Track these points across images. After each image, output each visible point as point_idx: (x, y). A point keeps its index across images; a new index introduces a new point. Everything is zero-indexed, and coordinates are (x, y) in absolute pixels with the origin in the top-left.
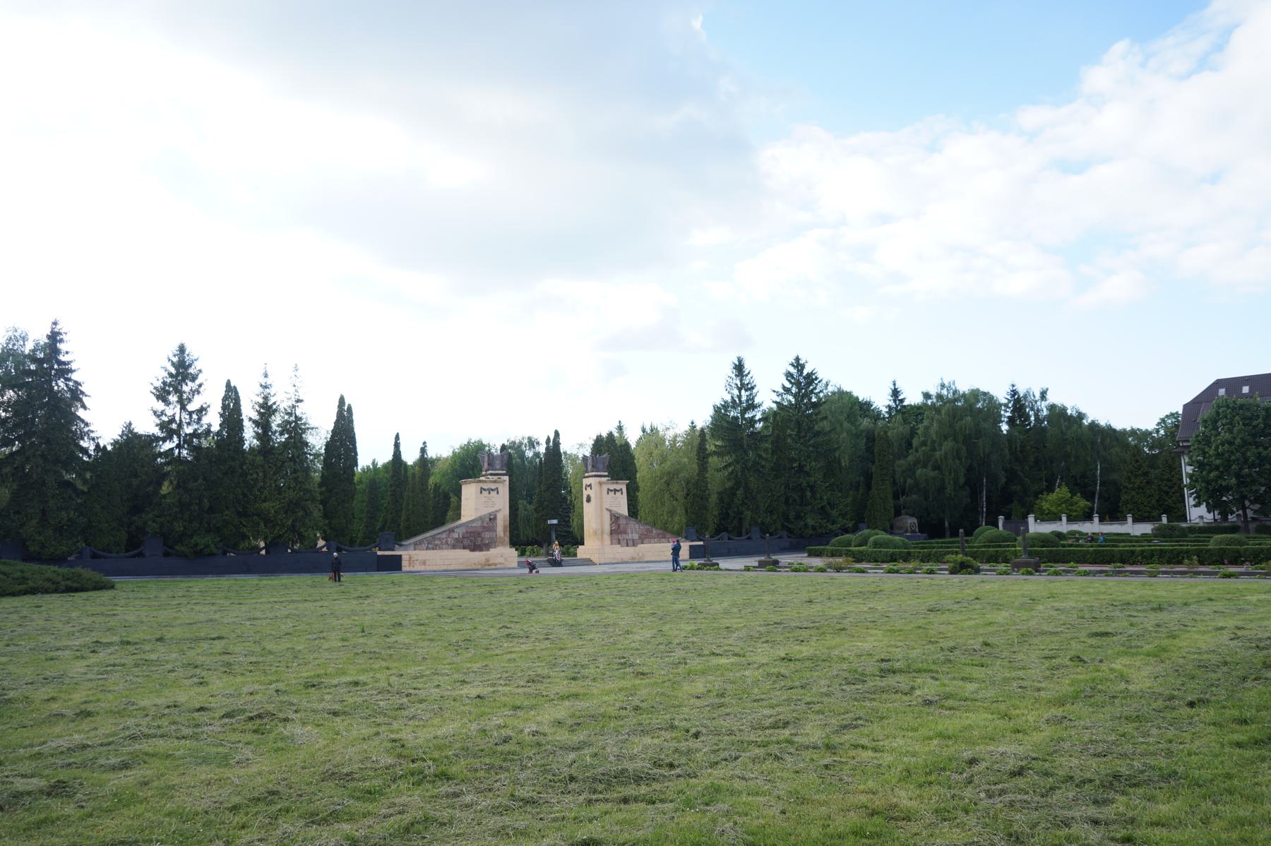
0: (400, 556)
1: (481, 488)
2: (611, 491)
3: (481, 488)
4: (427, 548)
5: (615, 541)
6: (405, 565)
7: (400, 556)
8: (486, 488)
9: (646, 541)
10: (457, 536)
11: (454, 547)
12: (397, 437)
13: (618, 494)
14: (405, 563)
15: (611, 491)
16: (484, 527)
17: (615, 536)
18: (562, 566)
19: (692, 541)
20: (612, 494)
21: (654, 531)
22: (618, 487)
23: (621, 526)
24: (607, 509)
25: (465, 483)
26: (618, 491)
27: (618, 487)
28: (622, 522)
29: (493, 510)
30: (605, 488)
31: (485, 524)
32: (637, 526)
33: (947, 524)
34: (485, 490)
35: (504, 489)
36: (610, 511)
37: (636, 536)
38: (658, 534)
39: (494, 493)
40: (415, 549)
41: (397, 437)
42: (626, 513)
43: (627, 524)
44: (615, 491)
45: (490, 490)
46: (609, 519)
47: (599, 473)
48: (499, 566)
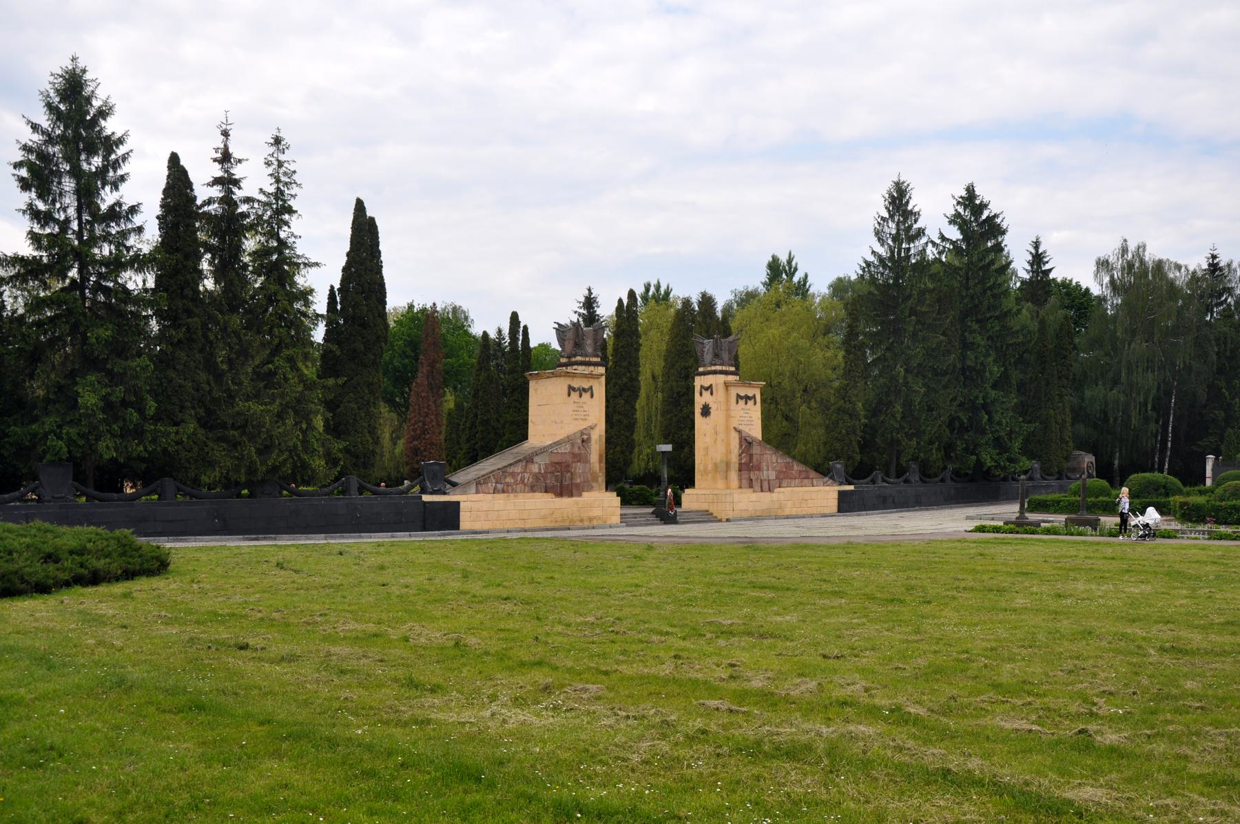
0: (458, 503)
2: (741, 398)
4: (495, 491)
5: (745, 482)
6: (466, 522)
7: (458, 503)
9: (785, 483)
10: (537, 471)
11: (533, 489)
14: (464, 516)
15: (741, 398)
16: (574, 455)
17: (745, 474)
18: (676, 522)
19: (841, 484)
20: (742, 402)
21: (795, 467)
22: (750, 392)
24: (735, 428)
25: (538, 377)
28: (756, 450)
29: (583, 425)
30: (734, 392)
31: (576, 450)
32: (774, 458)
33: (1116, 462)
34: (574, 389)
35: (600, 388)
36: (739, 432)
38: (800, 471)
39: (586, 396)
40: (477, 492)
42: (759, 437)
44: (747, 398)
46: (738, 446)
48: (595, 523)
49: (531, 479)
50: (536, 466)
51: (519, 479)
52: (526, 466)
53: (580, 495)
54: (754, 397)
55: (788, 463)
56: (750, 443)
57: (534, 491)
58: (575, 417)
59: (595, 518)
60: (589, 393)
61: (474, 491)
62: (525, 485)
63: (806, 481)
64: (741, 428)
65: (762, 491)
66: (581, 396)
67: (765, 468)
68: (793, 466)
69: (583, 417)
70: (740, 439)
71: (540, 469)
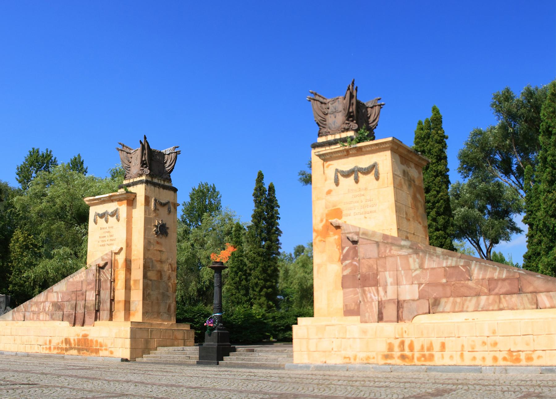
2: (347, 175)
15: (347, 175)
26: (366, 171)
27: (364, 161)
29: (107, 250)
42: (395, 233)
43: (381, 257)
44: (354, 173)
49: (51, 308)
51: (42, 308)
55: (456, 267)
56: (355, 242)
57: (54, 320)
58: (101, 243)
61: (11, 318)
63: (515, 299)
65: (380, 318)
67: (390, 280)
69: (109, 243)
71: (58, 298)
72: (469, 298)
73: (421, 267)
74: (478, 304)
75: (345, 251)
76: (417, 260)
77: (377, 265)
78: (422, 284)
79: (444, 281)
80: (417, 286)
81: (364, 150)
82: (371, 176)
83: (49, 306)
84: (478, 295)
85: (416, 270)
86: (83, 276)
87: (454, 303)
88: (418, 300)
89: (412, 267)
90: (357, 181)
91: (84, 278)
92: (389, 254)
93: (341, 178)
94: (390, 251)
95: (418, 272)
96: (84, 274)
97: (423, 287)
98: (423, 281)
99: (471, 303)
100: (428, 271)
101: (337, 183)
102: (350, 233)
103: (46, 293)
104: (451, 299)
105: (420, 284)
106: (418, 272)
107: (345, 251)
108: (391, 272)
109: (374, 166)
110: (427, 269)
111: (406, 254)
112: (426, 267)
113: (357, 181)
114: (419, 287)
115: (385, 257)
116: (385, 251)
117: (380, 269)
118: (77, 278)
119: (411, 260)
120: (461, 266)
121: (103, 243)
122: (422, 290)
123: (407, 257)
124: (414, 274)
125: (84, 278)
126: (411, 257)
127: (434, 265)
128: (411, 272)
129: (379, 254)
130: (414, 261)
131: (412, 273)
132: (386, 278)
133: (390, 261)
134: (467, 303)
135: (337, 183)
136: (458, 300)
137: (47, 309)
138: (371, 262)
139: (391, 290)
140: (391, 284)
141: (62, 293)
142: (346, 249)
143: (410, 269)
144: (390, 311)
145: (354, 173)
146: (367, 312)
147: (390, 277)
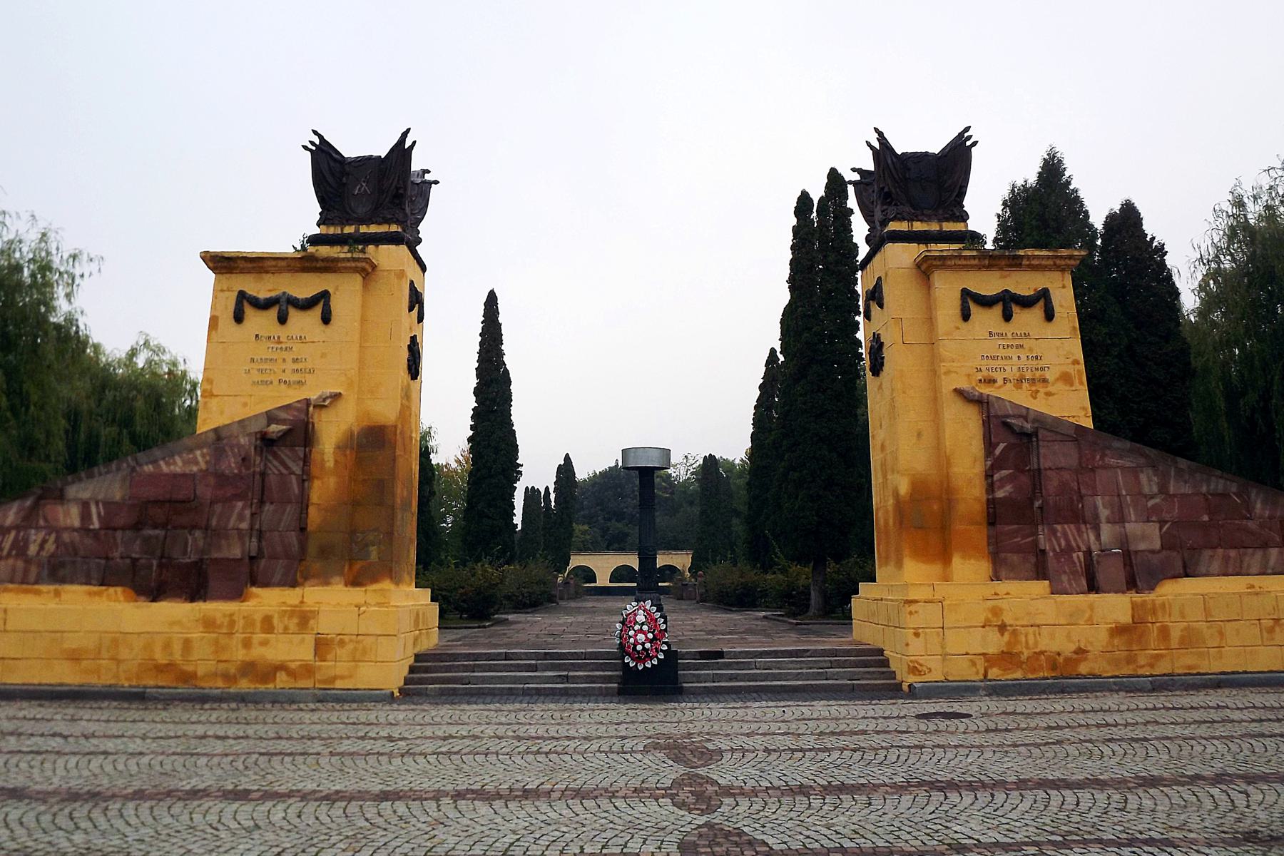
1: (242, 296)
2: (986, 302)
3: (242, 296)
8: (263, 295)
12: (491, 302)
13: (1028, 319)
15: (986, 302)
20: (985, 319)
23: (1052, 484)
24: (959, 392)
26: (1026, 303)
27: (1025, 284)
28: (1053, 457)
29: (292, 396)
30: (947, 288)
31: (231, 464)
32: (1148, 482)
36: (981, 402)
37: (1146, 536)
41: (491, 302)
42: (1089, 423)
43: (1085, 469)
45: (283, 307)
47: (918, 226)
50: (75, 511)
52: (36, 505)
53: (237, 594)
54: (1044, 295)
55: (1225, 495)
57: (63, 581)
58: (258, 377)
59: (282, 667)
60: (317, 311)
62: (28, 561)
64: (986, 390)
65: (1093, 587)
66: (283, 319)
67: (1104, 513)
68: (1249, 507)
70: (987, 424)
71: (85, 516)
72: (1250, 551)
73: (1163, 489)
74: (1266, 559)
75: (998, 452)
76: (1155, 479)
77: (1078, 484)
78: (1166, 522)
79: (1206, 518)
80: (1157, 525)
81: (1025, 262)
82: (1037, 312)
83: (44, 541)
84: (1265, 546)
85: (1152, 497)
86: (200, 459)
87: (1226, 559)
88: (1159, 552)
89: (1146, 490)
90: (1007, 317)
91: (203, 466)
92: (1100, 463)
93: (974, 308)
94: (1102, 458)
95: (1157, 500)
96: (203, 456)
97: (1168, 529)
98: (1167, 516)
99: (1255, 559)
100: (1176, 499)
101: (966, 316)
102: (1008, 416)
103: (28, 503)
104: (1220, 551)
105: (1162, 523)
106: (1157, 500)
107: (998, 452)
108: (1107, 498)
109: (1044, 295)
110: (1174, 495)
111: (1134, 465)
112: (1172, 490)
113: (1007, 317)
114: (1161, 529)
115: (1093, 470)
116: (1094, 458)
117: (1083, 491)
118: (175, 463)
119: (1143, 478)
120: (1234, 494)
121: (266, 378)
122: (1166, 532)
123: (1135, 472)
124: (1150, 503)
125: (203, 466)
126: (1142, 472)
127: (1187, 489)
128: (1144, 500)
129: (1080, 463)
130: (1150, 480)
131: (1147, 501)
132: (1096, 508)
133: (1102, 476)
134: (1247, 559)
135: (966, 316)
136: (1233, 553)
137: (33, 549)
138: (1066, 476)
139: (1107, 531)
140: (1108, 522)
141: (108, 504)
142: (1002, 446)
143: (1140, 493)
144: (1111, 570)
145: (1008, 303)
146: (1065, 572)
147: (1105, 507)
